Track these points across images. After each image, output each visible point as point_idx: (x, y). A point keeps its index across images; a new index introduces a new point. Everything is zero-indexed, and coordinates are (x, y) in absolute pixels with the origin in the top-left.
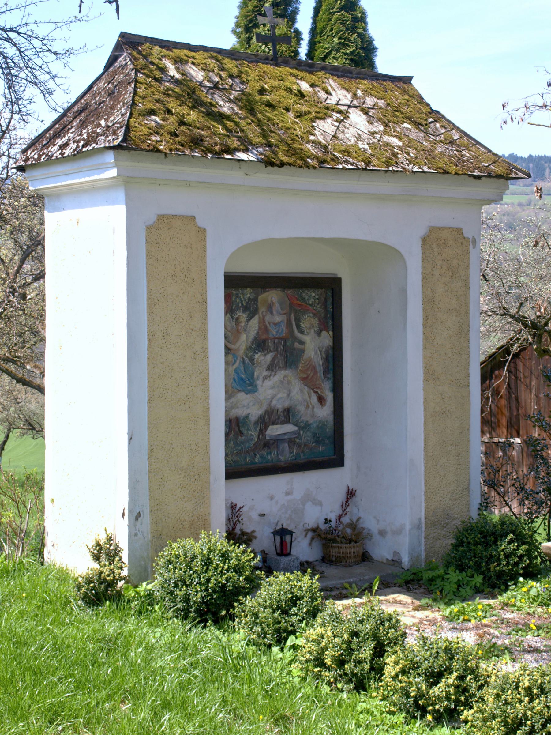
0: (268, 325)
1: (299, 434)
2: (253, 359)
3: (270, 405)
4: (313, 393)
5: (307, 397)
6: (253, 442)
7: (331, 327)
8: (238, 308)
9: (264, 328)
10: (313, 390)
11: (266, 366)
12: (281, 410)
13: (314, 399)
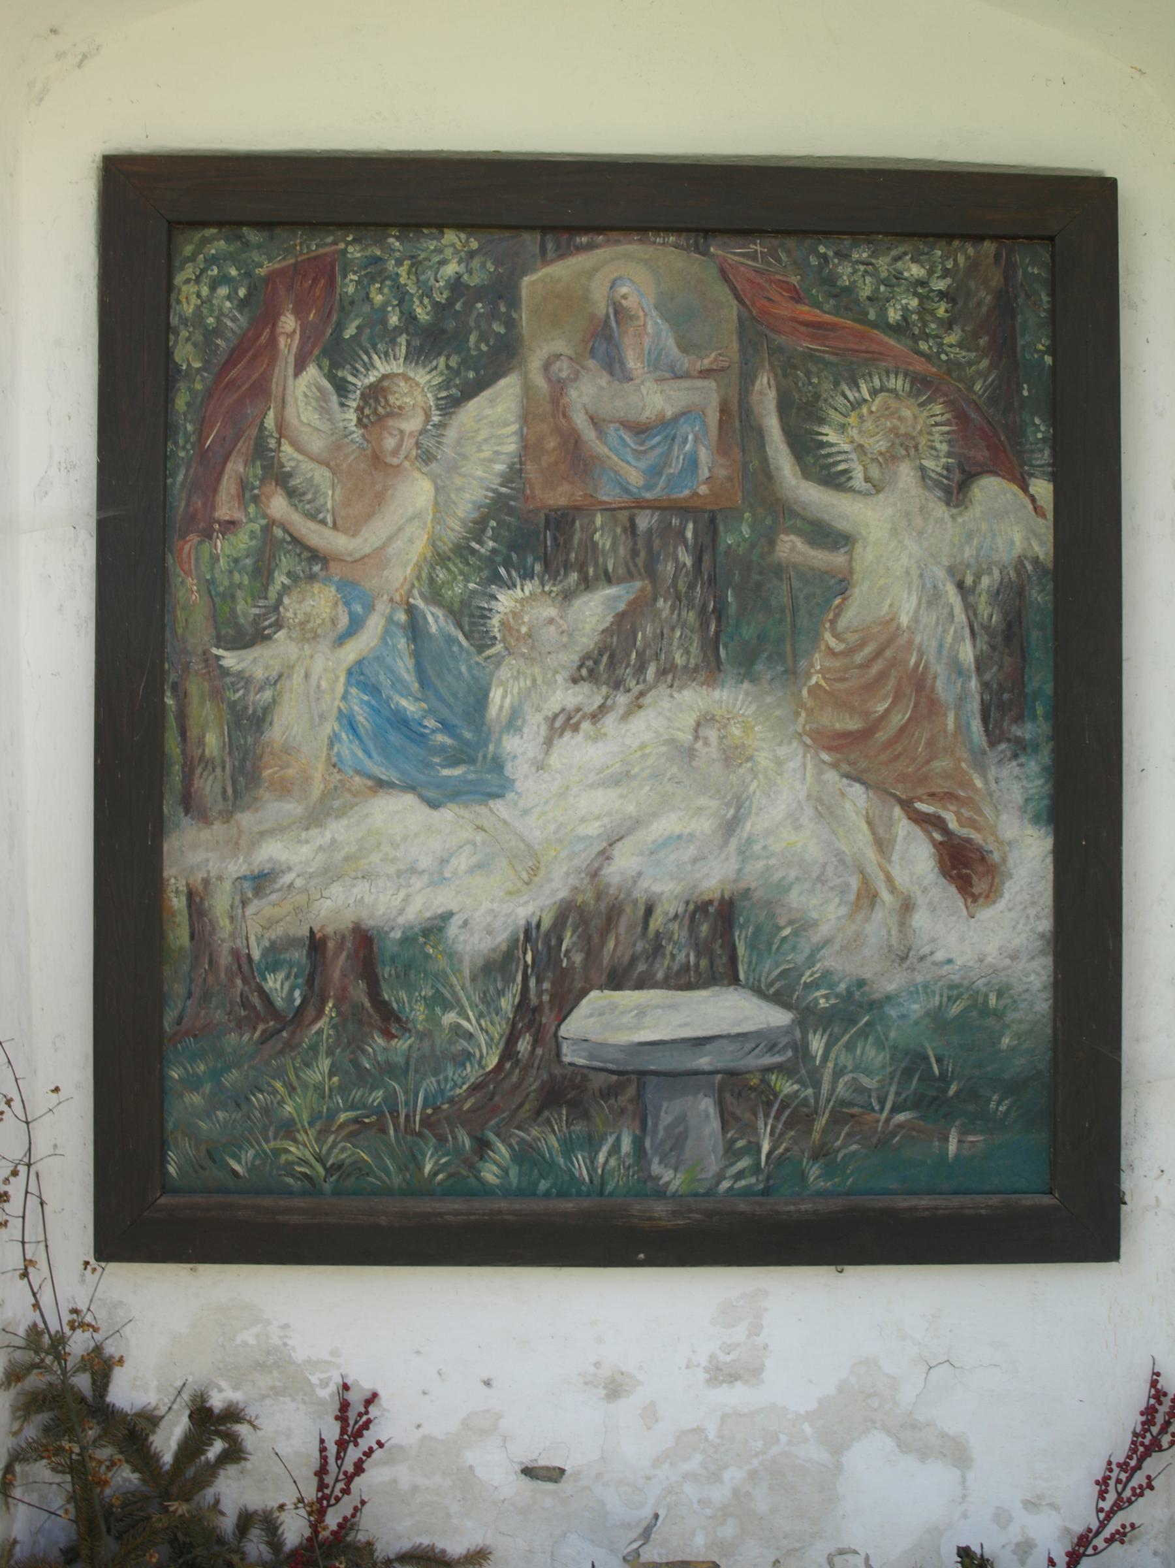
0: (589, 434)
1: (802, 1050)
2: (484, 615)
3: (595, 875)
4: (903, 826)
5: (861, 841)
6: (472, 1073)
7: (1044, 456)
8: (380, 336)
9: (555, 442)
10: (907, 805)
11: (570, 658)
12: (669, 907)
13: (916, 858)
